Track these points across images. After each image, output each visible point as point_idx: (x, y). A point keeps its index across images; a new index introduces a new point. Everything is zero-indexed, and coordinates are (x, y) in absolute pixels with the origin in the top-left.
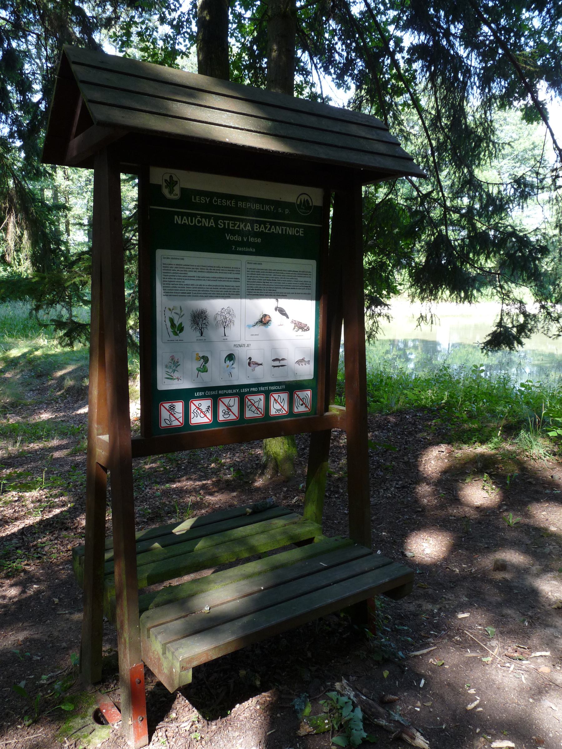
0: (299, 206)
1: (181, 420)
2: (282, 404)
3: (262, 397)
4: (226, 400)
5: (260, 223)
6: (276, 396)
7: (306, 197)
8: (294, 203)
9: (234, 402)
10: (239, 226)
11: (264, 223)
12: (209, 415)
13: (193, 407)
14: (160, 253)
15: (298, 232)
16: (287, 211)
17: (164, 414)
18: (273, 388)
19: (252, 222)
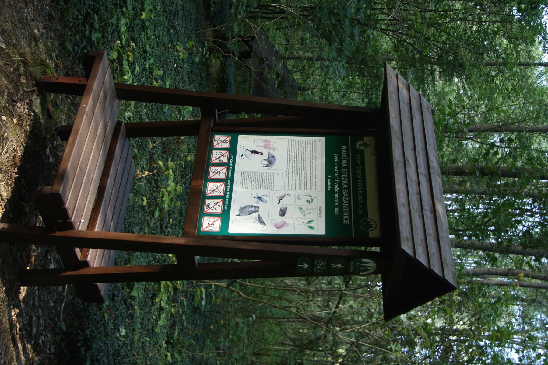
0: (366, 221)
1: (217, 146)
2: (213, 208)
3: (222, 194)
4: (224, 171)
5: (349, 193)
6: (220, 204)
7: (374, 226)
8: (367, 217)
9: (223, 176)
10: (344, 180)
11: (349, 196)
12: (217, 161)
13: (223, 152)
14: (323, 139)
15: (346, 220)
16: (360, 212)
17: (223, 138)
18: (227, 202)
19: (348, 188)
